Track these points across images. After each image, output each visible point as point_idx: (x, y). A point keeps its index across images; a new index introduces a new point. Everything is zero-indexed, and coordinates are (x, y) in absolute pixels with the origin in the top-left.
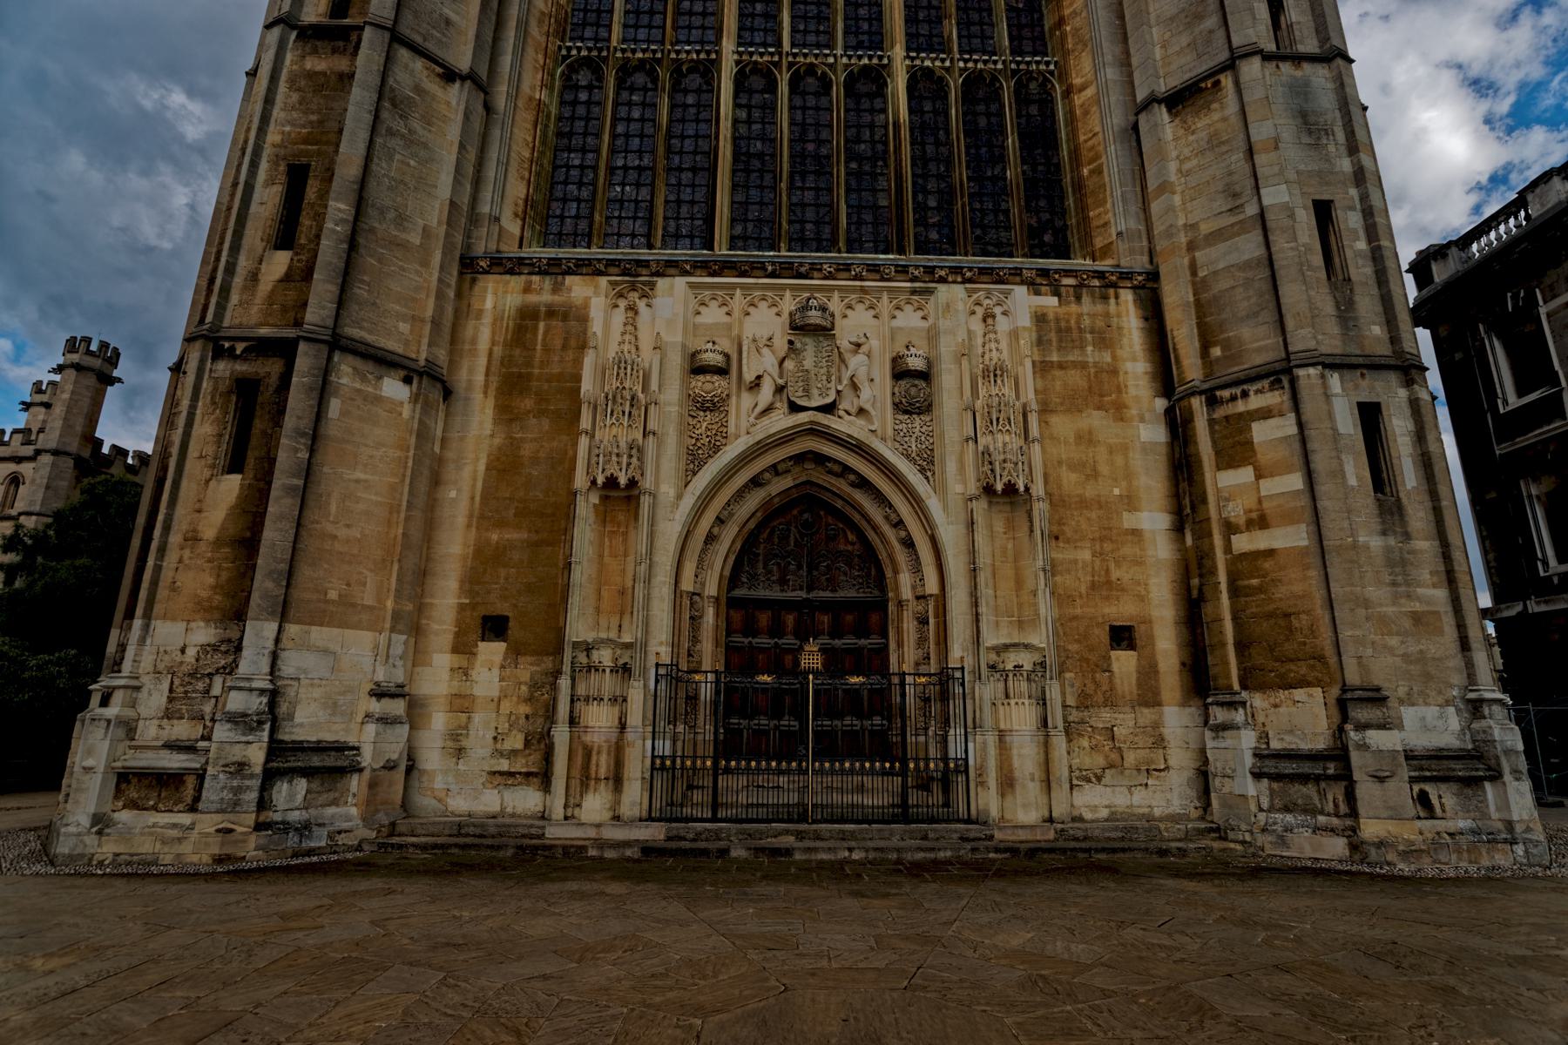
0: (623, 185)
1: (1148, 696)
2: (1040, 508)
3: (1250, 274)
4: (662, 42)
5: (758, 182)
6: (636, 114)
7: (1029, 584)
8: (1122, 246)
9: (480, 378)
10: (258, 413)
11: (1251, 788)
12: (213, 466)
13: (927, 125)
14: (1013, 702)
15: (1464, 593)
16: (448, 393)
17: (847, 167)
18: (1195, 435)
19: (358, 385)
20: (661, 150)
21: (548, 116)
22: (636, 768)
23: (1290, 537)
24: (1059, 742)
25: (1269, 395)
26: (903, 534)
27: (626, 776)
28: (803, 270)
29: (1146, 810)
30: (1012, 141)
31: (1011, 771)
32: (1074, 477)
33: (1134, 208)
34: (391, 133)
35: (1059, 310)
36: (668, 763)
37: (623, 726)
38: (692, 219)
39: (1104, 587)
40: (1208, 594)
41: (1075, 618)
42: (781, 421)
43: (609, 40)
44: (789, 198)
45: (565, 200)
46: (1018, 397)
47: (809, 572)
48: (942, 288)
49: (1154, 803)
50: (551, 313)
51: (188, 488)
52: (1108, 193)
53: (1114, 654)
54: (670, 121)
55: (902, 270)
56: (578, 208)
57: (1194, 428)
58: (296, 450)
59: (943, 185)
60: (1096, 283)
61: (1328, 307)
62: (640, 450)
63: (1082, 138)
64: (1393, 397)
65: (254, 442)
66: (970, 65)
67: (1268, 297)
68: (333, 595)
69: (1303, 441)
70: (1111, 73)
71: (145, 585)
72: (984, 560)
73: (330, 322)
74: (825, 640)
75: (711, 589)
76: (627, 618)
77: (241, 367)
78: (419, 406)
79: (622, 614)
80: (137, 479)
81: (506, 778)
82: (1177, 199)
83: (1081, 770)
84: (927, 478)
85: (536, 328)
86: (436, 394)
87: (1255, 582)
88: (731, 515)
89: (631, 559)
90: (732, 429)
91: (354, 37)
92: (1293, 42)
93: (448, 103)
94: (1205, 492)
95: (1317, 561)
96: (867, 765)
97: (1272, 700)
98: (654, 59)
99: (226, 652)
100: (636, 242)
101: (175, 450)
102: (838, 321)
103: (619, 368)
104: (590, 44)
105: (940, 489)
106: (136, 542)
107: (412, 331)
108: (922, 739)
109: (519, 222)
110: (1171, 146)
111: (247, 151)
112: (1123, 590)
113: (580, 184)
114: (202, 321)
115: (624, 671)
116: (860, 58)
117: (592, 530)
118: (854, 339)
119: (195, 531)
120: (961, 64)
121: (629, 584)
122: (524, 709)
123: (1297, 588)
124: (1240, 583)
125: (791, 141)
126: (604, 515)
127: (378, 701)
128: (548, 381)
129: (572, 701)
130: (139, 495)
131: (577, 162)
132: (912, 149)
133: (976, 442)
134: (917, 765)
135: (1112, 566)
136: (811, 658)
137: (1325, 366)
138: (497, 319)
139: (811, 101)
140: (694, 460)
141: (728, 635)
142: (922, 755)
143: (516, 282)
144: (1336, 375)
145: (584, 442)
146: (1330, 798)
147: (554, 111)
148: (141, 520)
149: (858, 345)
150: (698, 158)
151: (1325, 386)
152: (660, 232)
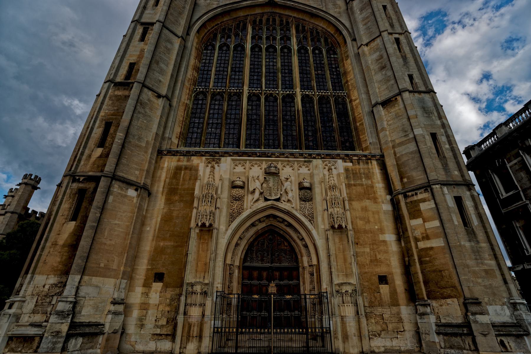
0: (212, 128)
2: (351, 233)
3: (413, 155)
4: (226, 87)
5: (255, 128)
6: (217, 107)
7: (349, 260)
8: (372, 147)
10: (85, 201)
12: (66, 219)
14: (345, 305)
15: (501, 262)
16: (150, 194)
17: (283, 123)
18: (401, 208)
19: (119, 191)
20: (224, 118)
21: (189, 108)
22: (207, 332)
23: (437, 243)
24: (364, 321)
25: (424, 194)
26: (304, 243)
27: (203, 335)
28: (269, 155)
29: (398, 348)
30: (334, 115)
31: (347, 332)
32: (361, 222)
33: (374, 135)
34: (139, 112)
35: (353, 167)
36: (220, 330)
37: (203, 315)
38: (233, 139)
39: (375, 261)
40: (412, 264)
41: (366, 273)
42: (262, 204)
43: (209, 86)
44: (264, 132)
45: (193, 133)
46: (341, 196)
47: (272, 256)
48: (314, 161)
49: (401, 345)
50: (186, 168)
51: (56, 226)
52: (366, 131)
53: (380, 286)
54: (227, 110)
55: (301, 155)
56: (197, 135)
57: (400, 206)
58: (96, 213)
59: (313, 129)
60: (364, 158)
61: (439, 165)
62: (214, 214)
63: (356, 115)
64: (466, 195)
65: (82, 210)
66: (320, 93)
67: (420, 162)
68: (102, 265)
69: (438, 209)
70: (364, 96)
71: (35, 261)
72: (332, 252)
73: (113, 171)
74: (277, 281)
75: (237, 263)
76: (207, 274)
77: (81, 185)
78: (139, 198)
79: (205, 272)
80: (39, 222)
81: (158, 337)
82: (388, 133)
83: (372, 332)
84: (312, 223)
85: (181, 173)
86: (146, 195)
87: (428, 259)
88: (244, 236)
89: (209, 252)
90: (245, 207)
91: (131, 86)
92: (417, 88)
93: (158, 104)
94: (406, 227)
95: (448, 251)
96: (293, 330)
97: (439, 303)
98: (223, 92)
99: (60, 287)
100: (215, 146)
101: (54, 213)
102: (281, 171)
103: (208, 186)
104: (203, 88)
105: (316, 227)
106: (34, 245)
107: (139, 174)
108: (313, 319)
109: (178, 139)
110: (384, 117)
111: (93, 118)
112: (382, 262)
113: (198, 128)
114: (70, 170)
115: (205, 294)
116: (286, 91)
117: (196, 242)
118: (286, 177)
119: (56, 241)
120: (318, 93)
121: (208, 261)
122: (167, 309)
123: (443, 261)
124: (422, 259)
125: (265, 115)
126: (200, 236)
127: (114, 305)
128: (184, 190)
129: (185, 306)
130: (38, 228)
131: (197, 121)
132: (303, 118)
133: (328, 211)
134: (312, 330)
135: (377, 253)
136: (272, 289)
137: (441, 184)
138: (168, 170)
139: (271, 104)
140: (232, 217)
141: (242, 280)
142: (313, 326)
143: (175, 158)
144: (445, 187)
145: (195, 211)
146: (467, 343)
147: (191, 106)
148: (38, 237)
149: (287, 179)
150: (236, 120)
151: (442, 191)
152: (223, 143)
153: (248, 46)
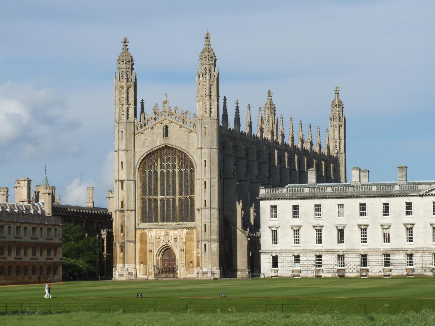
1: (193, 267)
9: (138, 240)
13: (180, 205)
24: (185, 271)
39: (190, 258)
42: (164, 244)
75: (160, 258)
81: (144, 275)
153: (159, 171)
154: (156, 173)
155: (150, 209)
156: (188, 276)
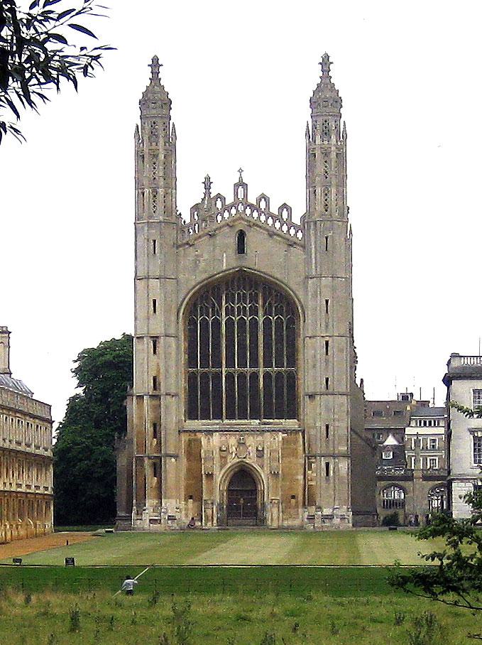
1: (297, 506)
11: (306, 520)
39: (291, 488)
42: (237, 460)
136: (242, 501)
140: (222, 467)
154: (217, 324)
155: (205, 393)
156: (286, 524)
